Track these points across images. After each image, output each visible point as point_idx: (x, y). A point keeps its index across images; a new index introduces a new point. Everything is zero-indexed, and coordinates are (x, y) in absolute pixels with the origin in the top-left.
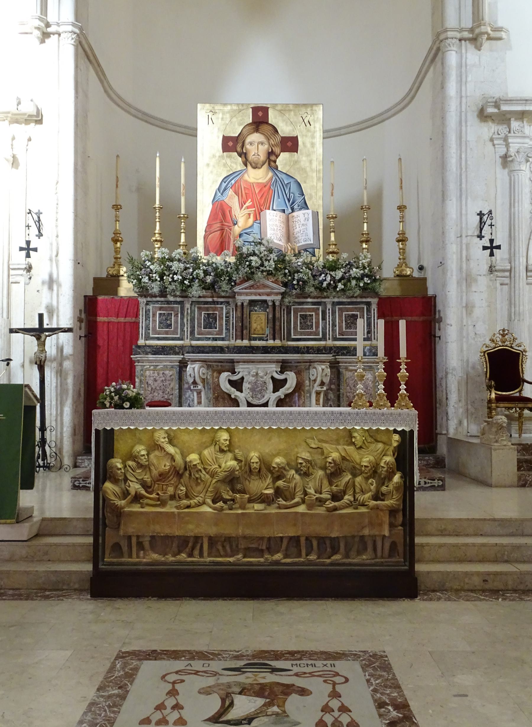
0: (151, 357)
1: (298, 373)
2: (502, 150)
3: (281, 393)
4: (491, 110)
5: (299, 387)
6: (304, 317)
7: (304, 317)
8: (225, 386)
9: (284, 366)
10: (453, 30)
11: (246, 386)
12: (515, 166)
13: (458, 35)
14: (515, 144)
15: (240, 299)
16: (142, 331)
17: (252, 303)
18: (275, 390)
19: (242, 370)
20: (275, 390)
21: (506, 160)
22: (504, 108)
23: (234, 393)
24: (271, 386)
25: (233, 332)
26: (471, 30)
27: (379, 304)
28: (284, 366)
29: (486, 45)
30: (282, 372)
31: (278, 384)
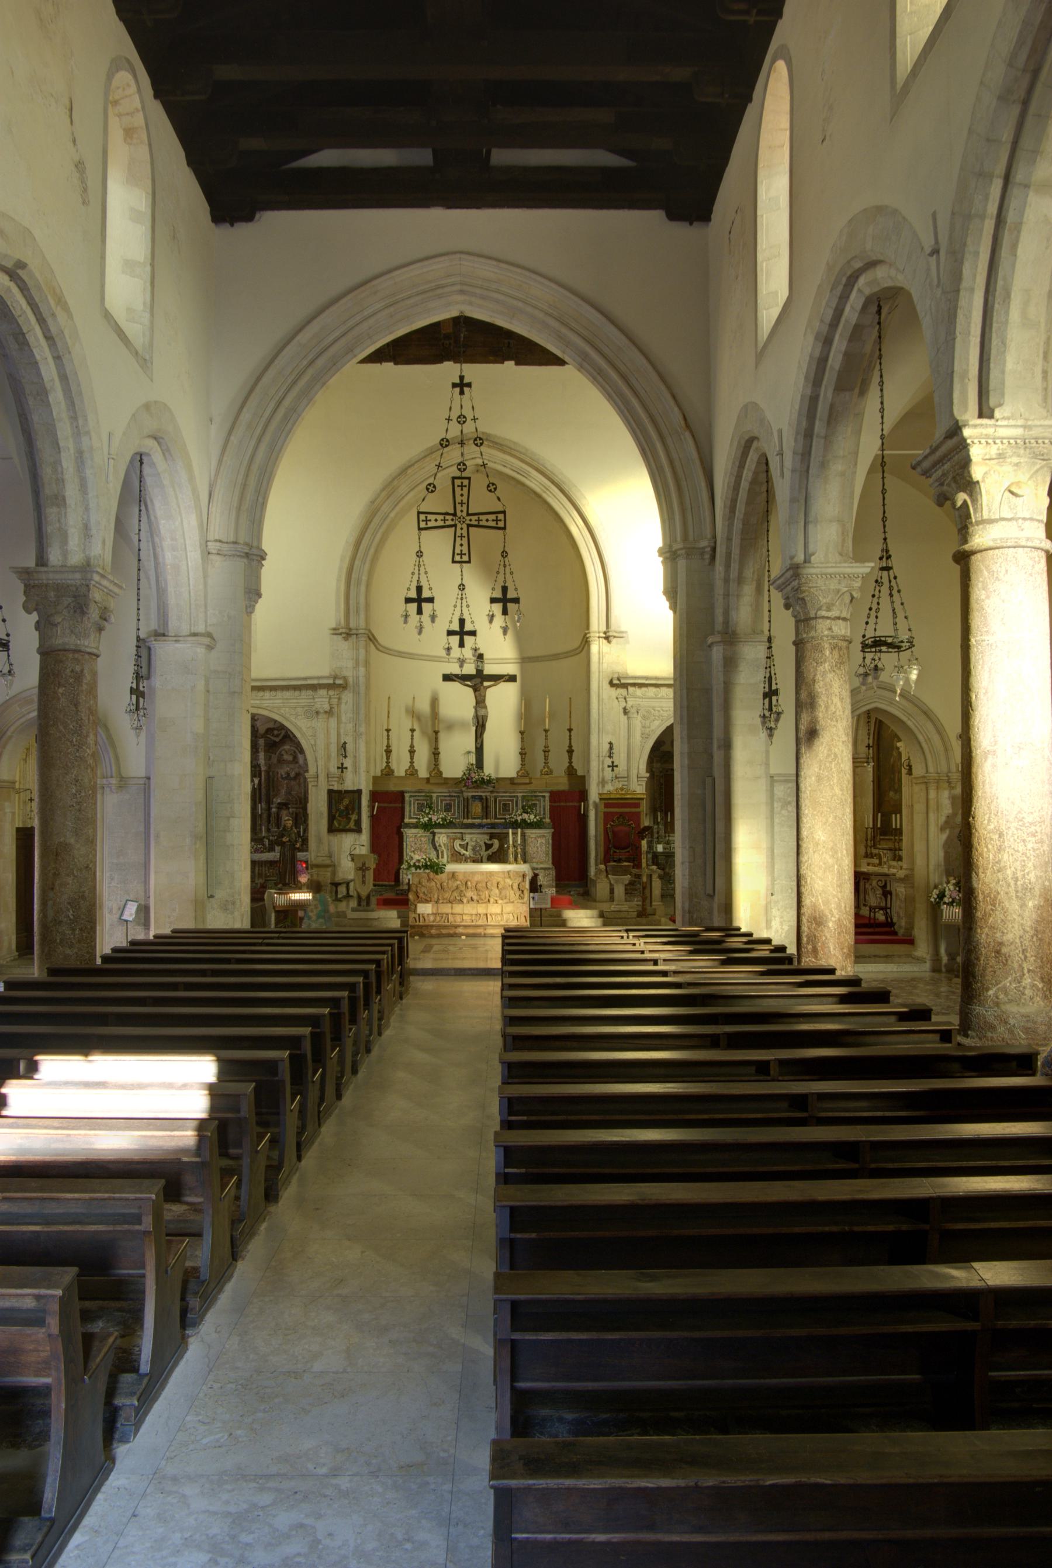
0: (414, 831)
1: (500, 840)
2: (623, 704)
3: (490, 852)
4: (615, 682)
5: (501, 847)
6: (505, 805)
7: (505, 805)
8: (458, 848)
9: (492, 836)
10: (595, 632)
11: (469, 847)
12: (630, 715)
13: (597, 635)
14: (631, 702)
15: (465, 794)
16: (407, 814)
17: (473, 797)
18: (487, 850)
19: (467, 838)
20: (487, 850)
21: (625, 711)
22: (623, 681)
23: (463, 851)
24: (484, 848)
25: (461, 814)
26: (605, 633)
27: (550, 797)
28: (492, 836)
29: (614, 641)
30: (490, 839)
31: (488, 847)
